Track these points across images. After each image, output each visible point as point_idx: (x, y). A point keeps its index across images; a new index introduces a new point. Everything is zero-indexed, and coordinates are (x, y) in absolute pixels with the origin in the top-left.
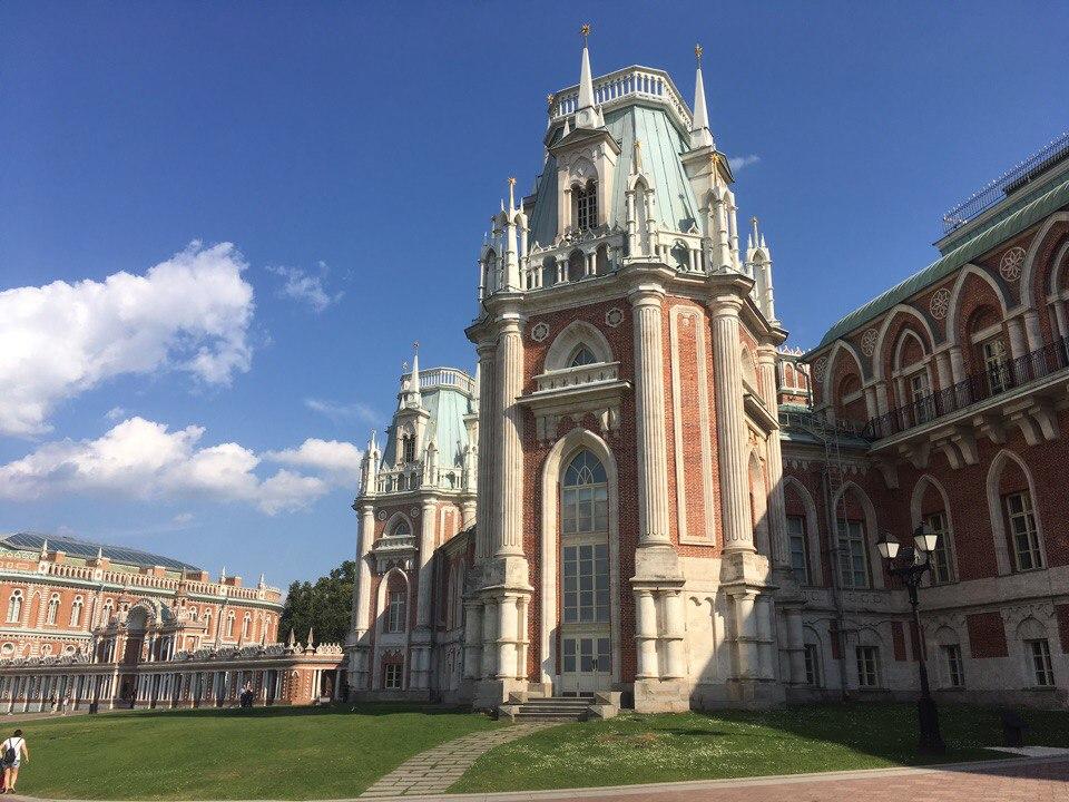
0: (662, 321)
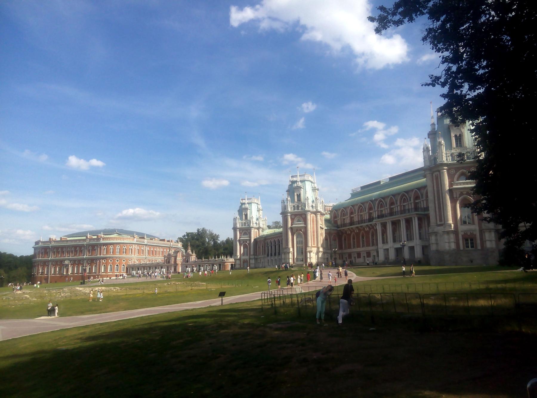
0: (310, 217)
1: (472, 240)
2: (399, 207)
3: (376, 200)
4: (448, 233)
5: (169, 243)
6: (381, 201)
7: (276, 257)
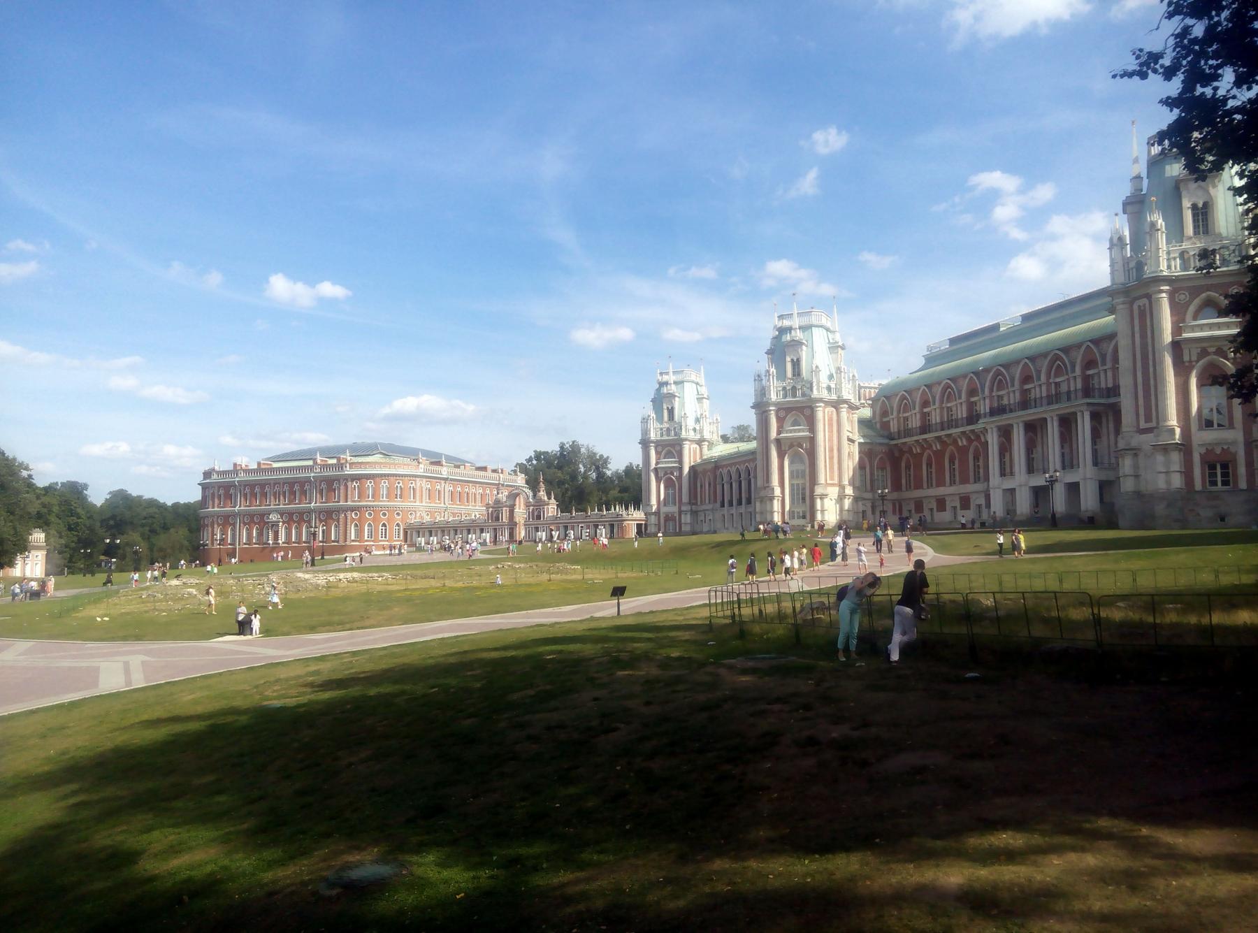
0: (823, 414)
1: (1225, 466)
2: (1044, 388)
3: (986, 371)
4: (1166, 449)
5: (495, 475)
6: (998, 373)
7: (742, 509)
